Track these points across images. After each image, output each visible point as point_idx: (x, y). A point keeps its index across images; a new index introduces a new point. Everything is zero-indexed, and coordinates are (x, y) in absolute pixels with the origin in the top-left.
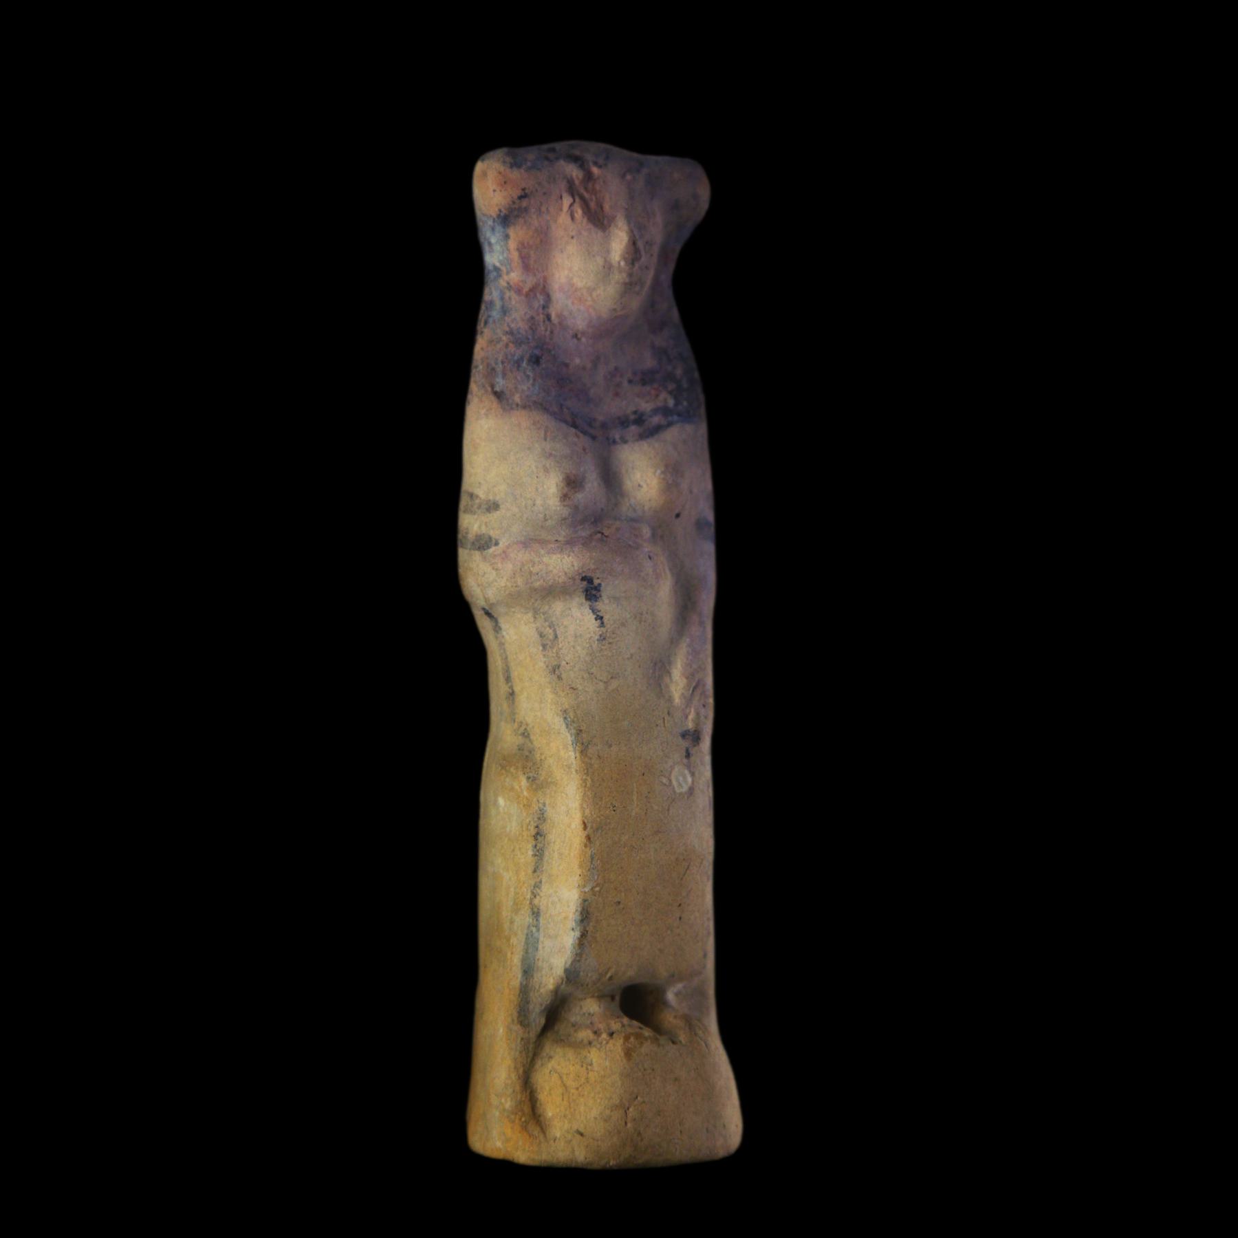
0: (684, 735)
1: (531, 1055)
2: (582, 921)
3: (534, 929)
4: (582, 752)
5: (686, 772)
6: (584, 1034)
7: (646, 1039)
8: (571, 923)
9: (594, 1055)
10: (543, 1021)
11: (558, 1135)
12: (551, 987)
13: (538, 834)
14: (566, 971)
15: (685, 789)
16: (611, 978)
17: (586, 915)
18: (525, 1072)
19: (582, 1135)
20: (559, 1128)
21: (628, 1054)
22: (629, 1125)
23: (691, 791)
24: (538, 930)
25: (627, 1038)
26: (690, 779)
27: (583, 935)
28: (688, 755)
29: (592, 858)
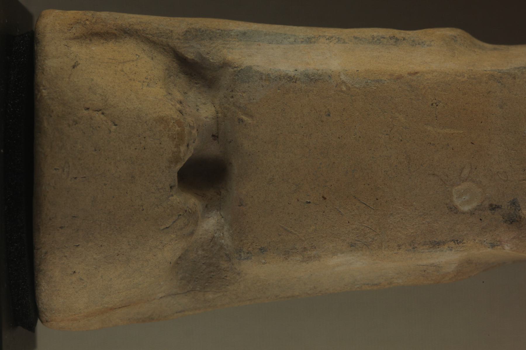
0: (514, 203)
1: (155, 39)
2: (307, 75)
3: (292, 40)
4: (493, 76)
5: (474, 205)
6: (179, 96)
7: (177, 146)
8: (301, 68)
9: (157, 91)
10: (190, 56)
11: (72, 49)
12: (230, 57)
13: (397, 40)
14: (250, 68)
15: (457, 202)
16: (241, 120)
17: (313, 79)
18: (137, 31)
19: (74, 67)
20: (78, 50)
21: (162, 120)
22: (86, 112)
23: (454, 210)
24: (291, 43)
25: (179, 123)
26: (466, 208)
27: (291, 79)
28: (493, 208)
29: (378, 81)
